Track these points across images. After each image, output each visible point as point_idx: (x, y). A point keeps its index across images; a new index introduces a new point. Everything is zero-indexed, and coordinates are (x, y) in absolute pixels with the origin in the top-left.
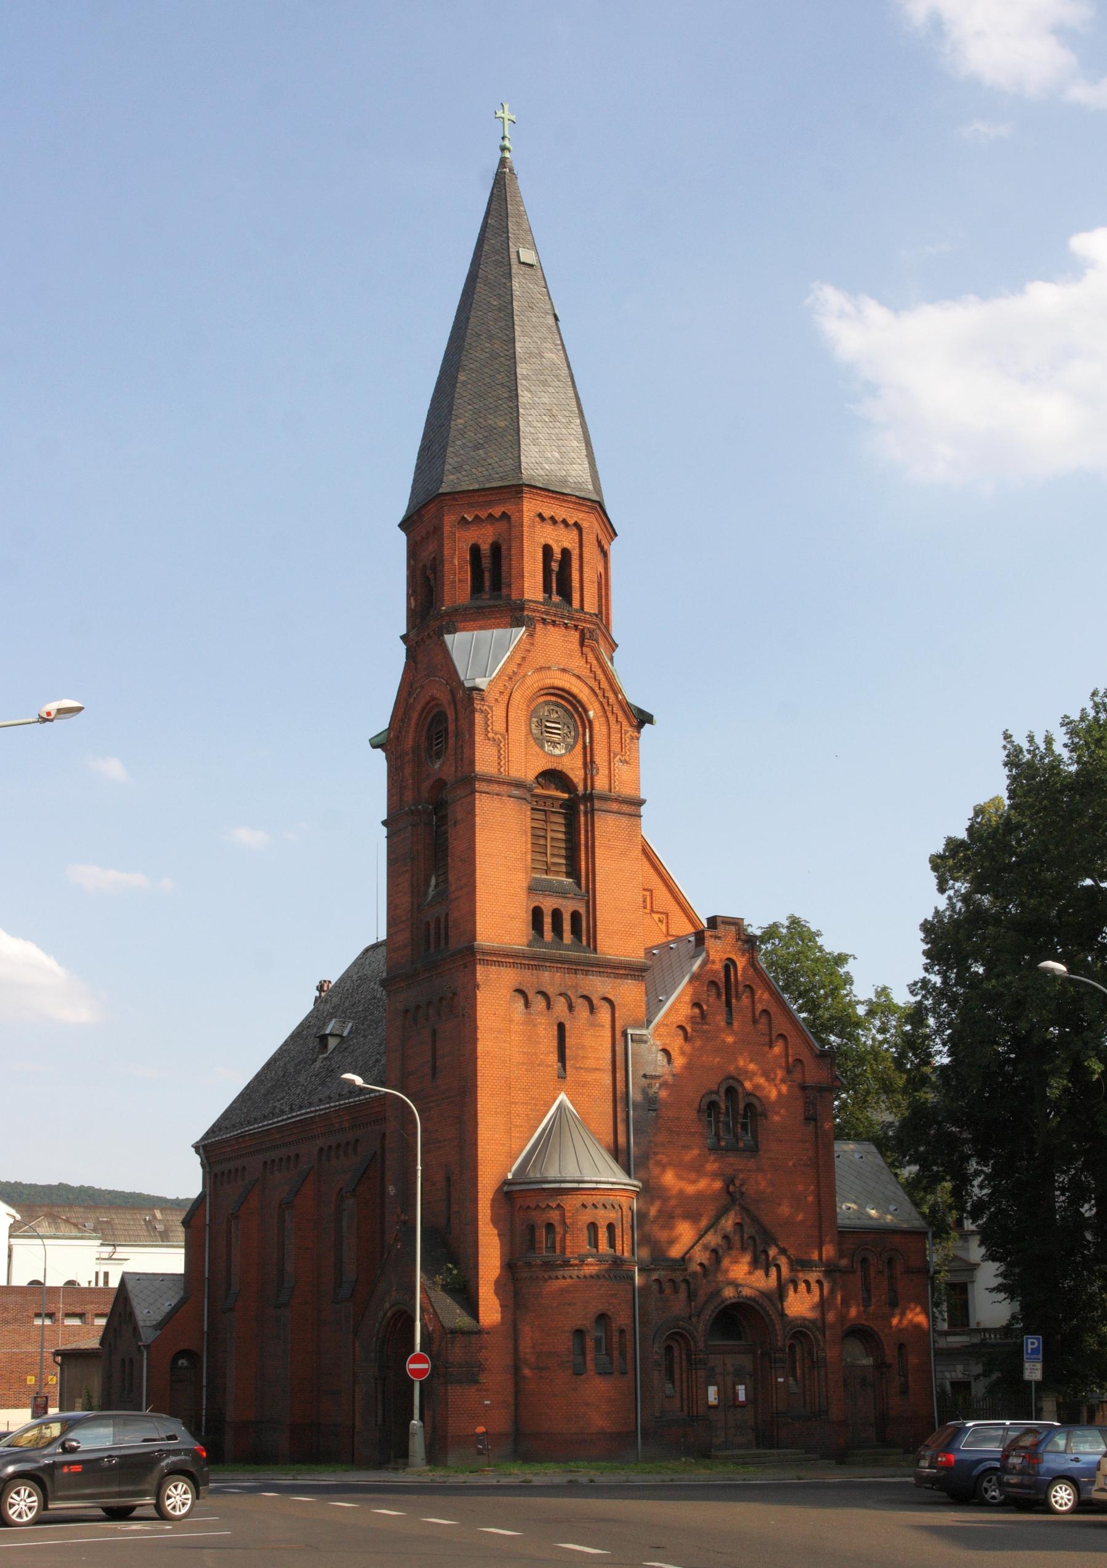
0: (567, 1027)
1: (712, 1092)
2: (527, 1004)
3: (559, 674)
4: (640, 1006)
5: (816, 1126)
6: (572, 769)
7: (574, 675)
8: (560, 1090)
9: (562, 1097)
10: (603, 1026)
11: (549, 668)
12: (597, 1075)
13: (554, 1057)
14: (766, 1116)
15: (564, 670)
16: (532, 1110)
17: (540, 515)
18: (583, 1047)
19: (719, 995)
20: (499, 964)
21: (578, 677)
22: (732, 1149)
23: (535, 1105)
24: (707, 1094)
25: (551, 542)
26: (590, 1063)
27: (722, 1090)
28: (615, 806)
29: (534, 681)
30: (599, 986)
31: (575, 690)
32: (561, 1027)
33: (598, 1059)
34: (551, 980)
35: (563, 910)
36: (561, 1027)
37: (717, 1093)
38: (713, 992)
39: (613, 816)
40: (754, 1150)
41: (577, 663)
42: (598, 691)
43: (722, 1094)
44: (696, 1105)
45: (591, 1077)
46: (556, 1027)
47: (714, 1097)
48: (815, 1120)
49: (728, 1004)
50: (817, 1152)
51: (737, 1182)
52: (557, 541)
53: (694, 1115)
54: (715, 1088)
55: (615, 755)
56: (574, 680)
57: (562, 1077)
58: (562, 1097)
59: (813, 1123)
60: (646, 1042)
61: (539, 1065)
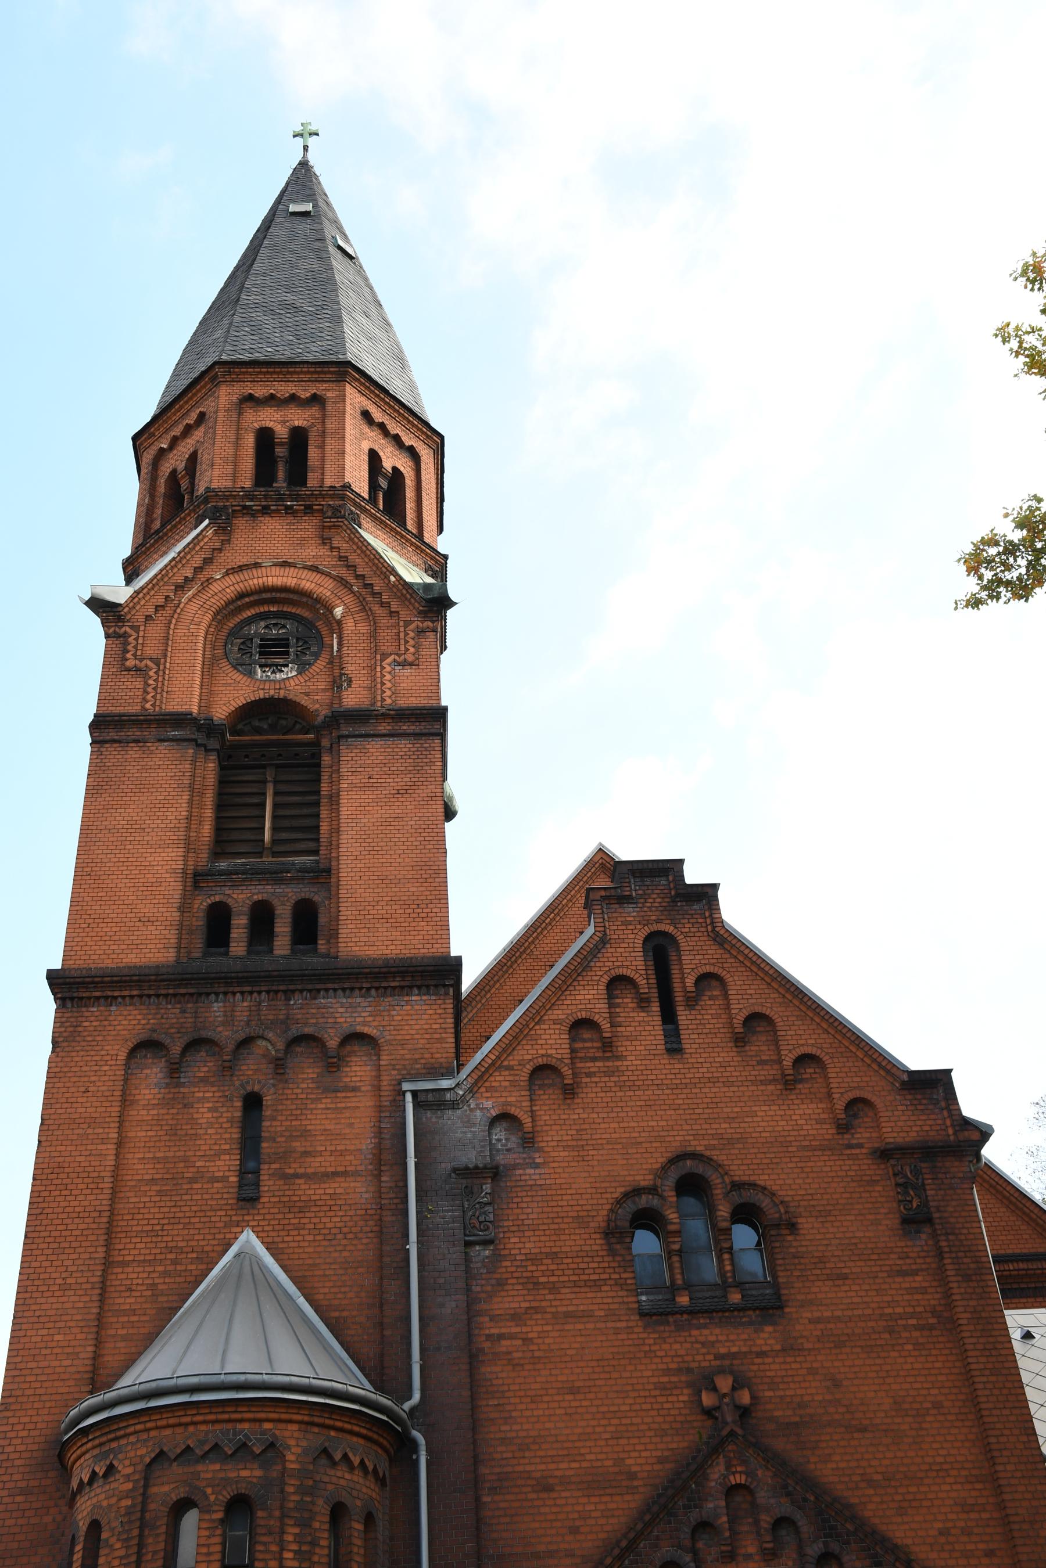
0: (268, 1100)
1: (637, 1192)
2: (174, 1071)
3: (276, 570)
4: (441, 1040)
5: (934, 1235)
6: (307, 694)
7: (305, 568)
8: (241, 1225)
9: (249, 1239)
10: (355, 1089)
11: (257, 565)
12: (337, 1186)
13: (227, 1165)
14: (793, 1227)
15: (285, 564)
16: (165, 1274)
17: (250, 398)
18: (305, 1134)
19: (643, 1003)
20: (111, 1000)
21: (314, 569)
22: (711, 1308)
23: (175, 1262)
24: (626, 1195)
25: (270, 424)
26: (316, 1164)
27: (670, 1182)
28: (384, 728)
29: (225, 587)
30: (341, 1013)
31: (307, 585)
32: (253, 1103)
33: (342, 1153)
34: (223, 1016)
35: (275, 902)
36: (253, 1103)
37: (652, 1190)
38: (627, 1001)
39: (380, 742)
40: (768, 1305)
41: (314, 552)
42: (351, 579)
43: (671, 1195)
44: (600, 1220)
45: (316, 1192)
46: (239, 1104)
47: (644, 1201)
48: (929, 1221)
49: (669, 1016)
50: (948, 1295)
51: (724, 1384)
52: (284, 422)
53: (597, 1243)
54: (645, 1180)
55: (385, 656)
56: (305, 573)
57: (248, 1196)
58: (249, 1239)
59: (927, 1229)
60: (454, 1105)
61: (193, 1180)
